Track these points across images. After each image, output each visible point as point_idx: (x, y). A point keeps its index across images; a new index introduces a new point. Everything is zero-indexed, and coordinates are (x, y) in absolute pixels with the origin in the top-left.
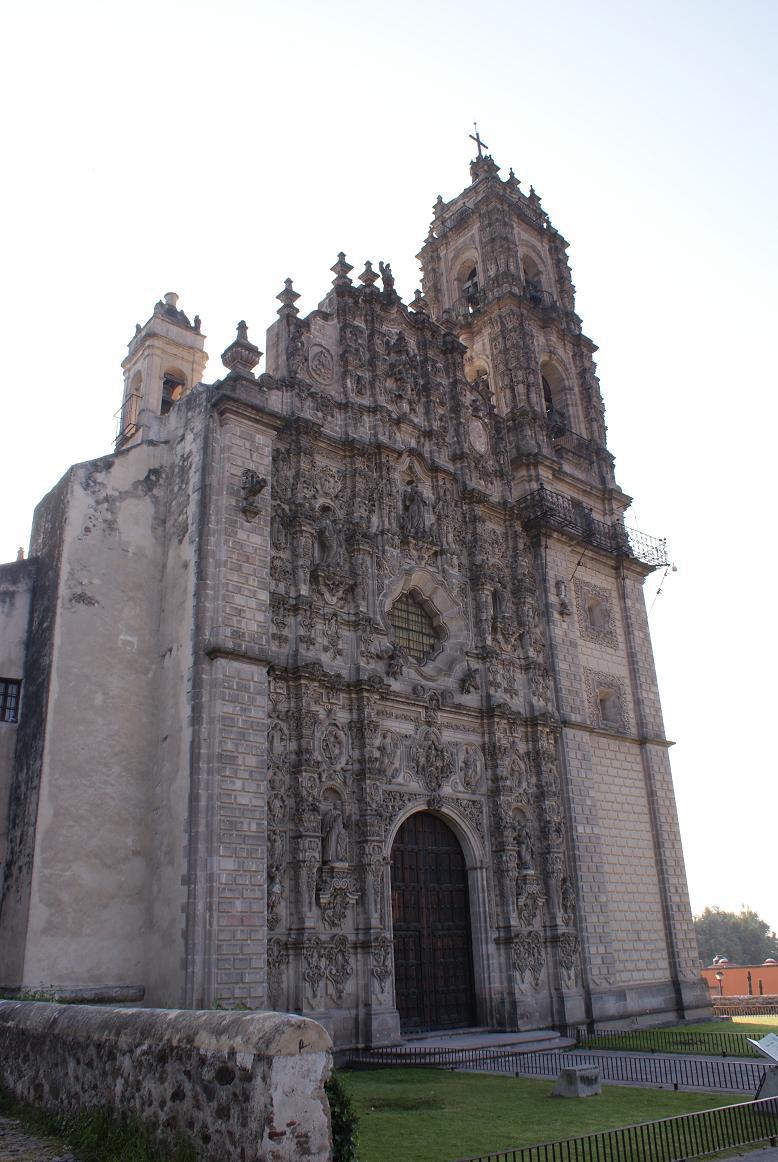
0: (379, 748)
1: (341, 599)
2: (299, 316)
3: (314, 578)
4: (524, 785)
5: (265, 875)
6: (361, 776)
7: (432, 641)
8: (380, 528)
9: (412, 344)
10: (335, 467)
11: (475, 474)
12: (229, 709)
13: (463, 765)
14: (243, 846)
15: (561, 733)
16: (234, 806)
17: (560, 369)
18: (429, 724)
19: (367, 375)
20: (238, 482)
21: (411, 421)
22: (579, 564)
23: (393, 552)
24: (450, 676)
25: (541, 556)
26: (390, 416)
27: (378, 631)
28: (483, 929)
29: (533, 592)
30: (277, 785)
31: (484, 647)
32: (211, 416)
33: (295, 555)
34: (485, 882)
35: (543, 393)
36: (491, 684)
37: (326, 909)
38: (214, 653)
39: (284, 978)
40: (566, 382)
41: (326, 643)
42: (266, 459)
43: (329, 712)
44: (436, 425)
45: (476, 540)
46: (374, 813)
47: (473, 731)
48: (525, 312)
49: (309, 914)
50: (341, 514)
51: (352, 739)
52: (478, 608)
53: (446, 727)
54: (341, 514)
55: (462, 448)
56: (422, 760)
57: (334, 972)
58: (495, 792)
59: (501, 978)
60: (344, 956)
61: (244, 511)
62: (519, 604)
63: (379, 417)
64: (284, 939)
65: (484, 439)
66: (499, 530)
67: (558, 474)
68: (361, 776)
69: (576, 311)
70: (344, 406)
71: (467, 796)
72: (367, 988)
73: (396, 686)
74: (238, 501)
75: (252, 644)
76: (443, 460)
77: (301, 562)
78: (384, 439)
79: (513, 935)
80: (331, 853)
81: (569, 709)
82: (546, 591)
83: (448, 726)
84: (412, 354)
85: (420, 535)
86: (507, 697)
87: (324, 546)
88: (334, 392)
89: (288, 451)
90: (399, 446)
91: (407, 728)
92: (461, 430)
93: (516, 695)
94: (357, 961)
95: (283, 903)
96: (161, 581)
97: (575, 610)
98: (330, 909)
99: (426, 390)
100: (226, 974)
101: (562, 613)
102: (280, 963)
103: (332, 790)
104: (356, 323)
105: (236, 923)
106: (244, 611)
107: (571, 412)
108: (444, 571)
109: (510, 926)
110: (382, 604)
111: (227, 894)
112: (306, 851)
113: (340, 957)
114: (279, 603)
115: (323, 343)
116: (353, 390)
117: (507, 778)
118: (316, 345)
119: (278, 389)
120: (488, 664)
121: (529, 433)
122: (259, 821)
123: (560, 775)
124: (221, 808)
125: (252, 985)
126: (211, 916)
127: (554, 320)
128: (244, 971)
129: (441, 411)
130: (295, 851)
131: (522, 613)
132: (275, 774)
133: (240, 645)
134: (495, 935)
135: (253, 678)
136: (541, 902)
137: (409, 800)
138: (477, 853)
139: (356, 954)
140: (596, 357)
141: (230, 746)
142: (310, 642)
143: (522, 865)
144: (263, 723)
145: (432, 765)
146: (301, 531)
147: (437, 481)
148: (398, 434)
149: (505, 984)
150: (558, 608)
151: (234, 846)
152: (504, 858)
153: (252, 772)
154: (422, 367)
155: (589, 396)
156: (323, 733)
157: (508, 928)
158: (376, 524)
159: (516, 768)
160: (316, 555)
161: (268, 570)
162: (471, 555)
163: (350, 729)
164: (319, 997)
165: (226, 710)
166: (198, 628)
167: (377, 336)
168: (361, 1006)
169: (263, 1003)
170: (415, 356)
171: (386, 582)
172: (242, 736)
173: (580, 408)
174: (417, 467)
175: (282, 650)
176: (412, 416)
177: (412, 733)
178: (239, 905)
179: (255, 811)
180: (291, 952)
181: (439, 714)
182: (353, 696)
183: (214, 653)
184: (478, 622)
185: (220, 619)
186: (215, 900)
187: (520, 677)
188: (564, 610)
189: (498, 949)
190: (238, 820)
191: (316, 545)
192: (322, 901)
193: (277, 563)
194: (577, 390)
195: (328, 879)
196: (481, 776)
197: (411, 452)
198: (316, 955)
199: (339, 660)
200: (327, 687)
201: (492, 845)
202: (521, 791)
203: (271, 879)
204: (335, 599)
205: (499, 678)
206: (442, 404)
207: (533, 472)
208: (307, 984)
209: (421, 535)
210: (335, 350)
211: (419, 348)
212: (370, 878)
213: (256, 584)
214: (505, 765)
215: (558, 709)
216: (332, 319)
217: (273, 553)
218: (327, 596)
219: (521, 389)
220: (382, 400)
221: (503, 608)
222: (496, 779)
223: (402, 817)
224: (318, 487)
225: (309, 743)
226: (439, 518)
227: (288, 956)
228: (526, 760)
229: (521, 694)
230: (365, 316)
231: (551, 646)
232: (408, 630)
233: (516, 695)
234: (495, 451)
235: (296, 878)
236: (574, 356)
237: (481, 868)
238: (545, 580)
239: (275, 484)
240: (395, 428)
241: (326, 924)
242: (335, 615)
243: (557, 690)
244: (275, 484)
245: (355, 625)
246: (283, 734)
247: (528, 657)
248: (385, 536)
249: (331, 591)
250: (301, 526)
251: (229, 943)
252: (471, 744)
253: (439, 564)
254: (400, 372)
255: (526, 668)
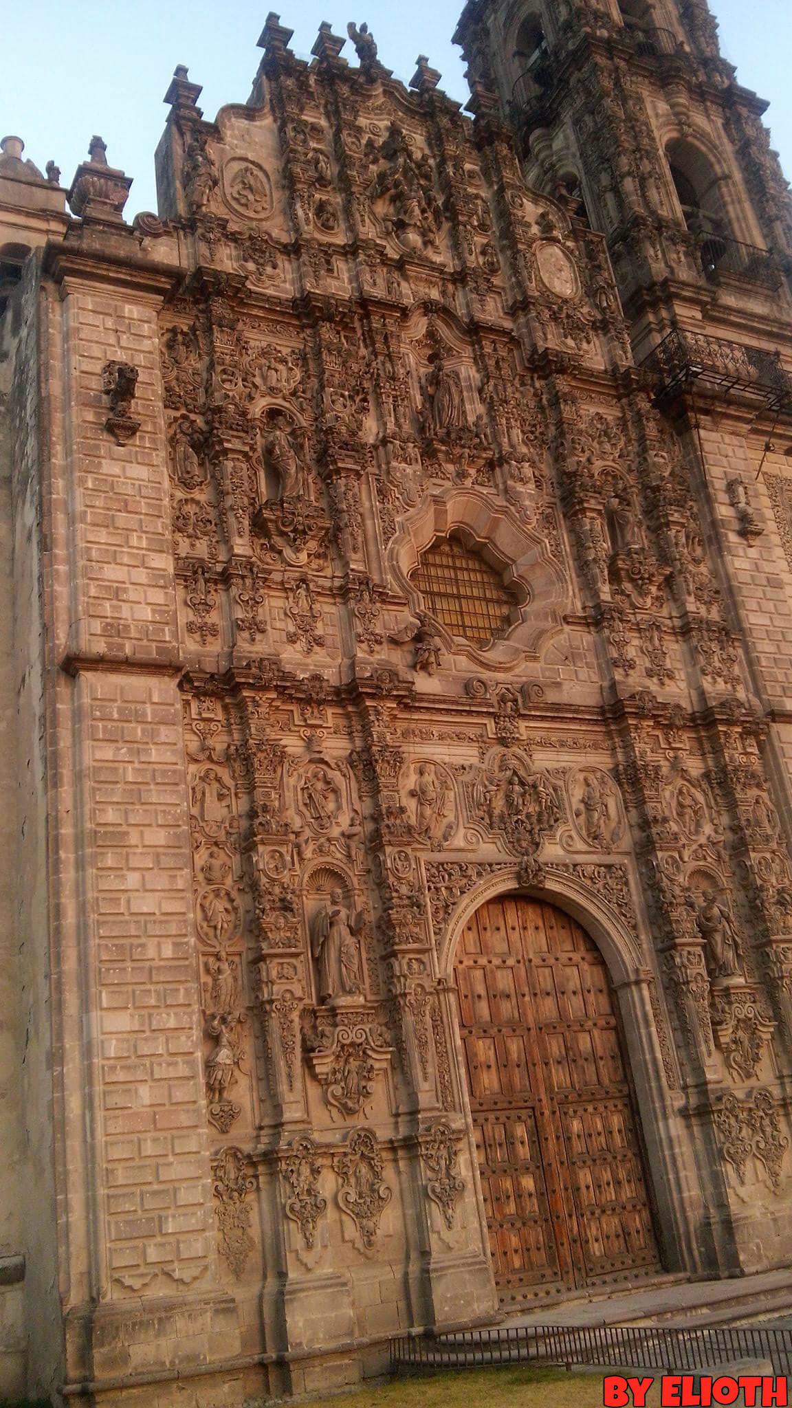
0: (412, 794)
1: (318, 556)
2: (204, 118)
3: (259, 527)
4: (708, 829)
5: (196, 1034)
6: (375, 844)
7: (505, 610)
8: (381, 435)
9: (418, 141)
10: (287, 344)
11: (552, 329)
12: (107, 753)
13: (582, 807)
14: (148, 987)
15: (768, 734)
16: (127, 918)
17: (703, 148)
18: (503, 742)
19: (338, 199)
20: (96, 384)
21: (427, 259)
22: (767, 448)
23: (408, 471)
24: (535, 659)
25: (694, 445)
26: (382, 254)
27: (384, 598)
28: (655, 1092)
29: (680, 503)
30: (216, 874)
31: (597, 607)
32: (43, 288)
33: (221, 494)
34: (648, 1008)
35: (673, 188)
36: (615, 664)
37: (328, 1084)
38: (72, 666)
39: (254, 1216)
40: (717, 168)
41: (292, 629)
42: (147, 342)
43: (309, 743)
44: (474, 260)
45: (562, 434)
46: (406, 902)
47: (596, 746)
48: (622, 64)
49: (288, 1097)
50: (303, 421)
51: (358, 782)
52: (579, 544)
53: (540, 744)
54: (303, 421)
55: (524, 293)
56: (499, 805)
57: (352, 1198)
58: (645, 849)
59: (700, 1178)
60: (372, 1167)
61: (111, 428)
62: (658, 527)
63: (362, 257)
64: (247, 1148)
65: (567, 274)
66: (611, 413)
67: (713, 313)
68: (375, 844)
69: (723, 54)
70: (293, 250)
71: (594, 858)
72: (420, 1222)
73: (425, 684)
74: (97, 414)
75: (145, 642)
76: (492, 311)
77: (230, 501)
78: (379, 292)
79: (712, 1097)
80: (331, 986)
81: (779, 691)
82: (709, 501)
83: (545, 744)
84: (418, 155)
85: (453, 436)
86: (653, 685)
87: (276, 475)
88: (278, 231)
89: (193, 329)
90: (408, 301)
91: (466, 754)
92: (521, 263)
93: (671, 677)
94: (399, 1173)
95: (244, 1083)
96: (12, 573)
97: (771, 526)
98: (336, 1082)
99: (449, 213)
100: (126, 1222)
101: (743, 534)
102: (241, 1191)
103: (330, 872)
104: (308, 117)
105: (141, 1128)
106: (125, 590)
107: (732, 215)
108: (506, 491)
109: (706, 1083)
110: (393, 556)
111: (121, 1076)
112: (273, 983)
113: (364, 1169)
114: (195, 573)
115: (250, 156)
116: (307, 220)
117: (665, 820)
118: (234, 159)
119: (168, 233)
120: (607, 632)
121: (651, 252)
122: (178, 940)
123: (777, 805)
124: (100, 924)
125: (182, 1237)
126: (92, 1120)
127: (678, 69)
128: (163, 1213)
129: (479, 240)
130: (256, 985)
131: (667, 543)
132: (211, 855)
133: (121, 647)
134: (676, 1100)
135: (150, 696)
136: (766, 1033)
137: (479, 874)
138: (626, 957)
139: (395, 1161)
140: (766, 119)
141: (111, 816)
142: (257, 628)
143: (716, 968)
144: (174, 772)
145: (518, 812)
146: (225, 452)
147: (482, 348)
148: (404, 284)
149: (710, 1189)
150: (736, 525)
151: (130, 988)
152: (678, 960)
153: (158, 855)
154: (440, 173)
155: (761, 181)
156: (300, 776)
157: (702, 1086)
158: (375, 430)
159: (688, 802)
160: (263, 488)
161: (168, 521)
162: (559, 458)
163: (351, 764)
164: (318, 1247)
165: (99, 755)
166: (47, 630)
167: (345, 132)
168: (413, 1255)
169: (206, 1268)
170: (425, 158)
171: (398, 519)
172: (136, 795)
173: (747, 206)
174: (444, 331)
175: (209, 648)
176: (430, 253)
177: (475, 761)
178: (146, 1094)
179: (166, 922)
180: (261, 1169)
181: (522, 724)
182: (350, 709)
183: (72, 666)
184: (583, 566)
185: (80, 608)
186: (99, 1088)
187: (674, 650)
188: (748, 529)
189: (689, 1127)
190: (136, 941)
191: (262, 474)
192: (318, 1070)
193: (191, 509)
194: (738, 176)
195: (328, 1029)
196: (619, 822)
197: (428, 307)
198: (305, 1170)
199: (320, 655)
200: (299, 700)
201: (655, 938)
202: (703, 840)
203: (213, 1039)
204: (303, 557)
205: (631, 652)
206: (483, 227)
207: (664, 314)
208: (292, 1225)
209: (457, 436)
210: (271, 164)
211: (430, 145)
212: (409, 1019)
213: (144, 544)
214: (664, 800)
215: (757, 693)
216: (262, 117)
217: (180, 495)
218: (288, 552)
219: (629, 185)
220: (369, 231)
221: (628, 537)
222: (645, 824)
223: (467, 907)
224: (258, 381)
225: (268, 795)
226: (491, 408)
227: (256, 1177)
228: (705, 786)
229: (681, 675)
230: (325, 107)
231: (731, 591)
232: (458, 597)
233: (671, 677)
234: (592, 292)
235: (262, 1035)
236: (726, 126)
237: (638, 983)
238: (705, 485)
239: (174, 383)
240: (396, 275)
241: (335, 1112)
242: (304, 581)
243: (751, 663)
244: (174, 383)
245: (342, 593)
246: (224, 786)
247: (686, 613)
248: (390, 446)
249: (292, 543)
250: (221, 442)
251: (131, 1164)
252: (593, 770)
253: (499, 480)
254: (397, 184)
255: (685, 631)
